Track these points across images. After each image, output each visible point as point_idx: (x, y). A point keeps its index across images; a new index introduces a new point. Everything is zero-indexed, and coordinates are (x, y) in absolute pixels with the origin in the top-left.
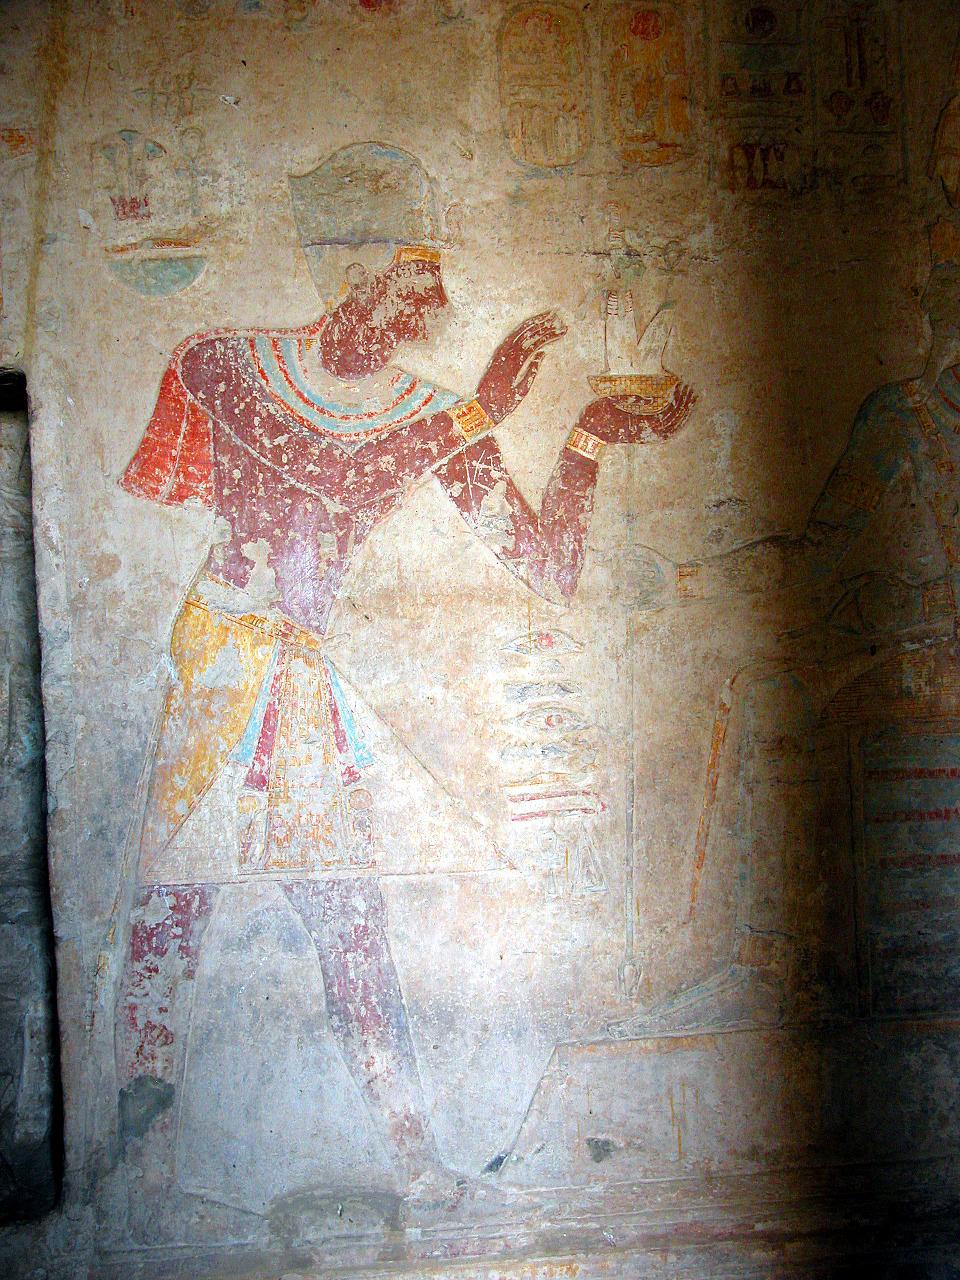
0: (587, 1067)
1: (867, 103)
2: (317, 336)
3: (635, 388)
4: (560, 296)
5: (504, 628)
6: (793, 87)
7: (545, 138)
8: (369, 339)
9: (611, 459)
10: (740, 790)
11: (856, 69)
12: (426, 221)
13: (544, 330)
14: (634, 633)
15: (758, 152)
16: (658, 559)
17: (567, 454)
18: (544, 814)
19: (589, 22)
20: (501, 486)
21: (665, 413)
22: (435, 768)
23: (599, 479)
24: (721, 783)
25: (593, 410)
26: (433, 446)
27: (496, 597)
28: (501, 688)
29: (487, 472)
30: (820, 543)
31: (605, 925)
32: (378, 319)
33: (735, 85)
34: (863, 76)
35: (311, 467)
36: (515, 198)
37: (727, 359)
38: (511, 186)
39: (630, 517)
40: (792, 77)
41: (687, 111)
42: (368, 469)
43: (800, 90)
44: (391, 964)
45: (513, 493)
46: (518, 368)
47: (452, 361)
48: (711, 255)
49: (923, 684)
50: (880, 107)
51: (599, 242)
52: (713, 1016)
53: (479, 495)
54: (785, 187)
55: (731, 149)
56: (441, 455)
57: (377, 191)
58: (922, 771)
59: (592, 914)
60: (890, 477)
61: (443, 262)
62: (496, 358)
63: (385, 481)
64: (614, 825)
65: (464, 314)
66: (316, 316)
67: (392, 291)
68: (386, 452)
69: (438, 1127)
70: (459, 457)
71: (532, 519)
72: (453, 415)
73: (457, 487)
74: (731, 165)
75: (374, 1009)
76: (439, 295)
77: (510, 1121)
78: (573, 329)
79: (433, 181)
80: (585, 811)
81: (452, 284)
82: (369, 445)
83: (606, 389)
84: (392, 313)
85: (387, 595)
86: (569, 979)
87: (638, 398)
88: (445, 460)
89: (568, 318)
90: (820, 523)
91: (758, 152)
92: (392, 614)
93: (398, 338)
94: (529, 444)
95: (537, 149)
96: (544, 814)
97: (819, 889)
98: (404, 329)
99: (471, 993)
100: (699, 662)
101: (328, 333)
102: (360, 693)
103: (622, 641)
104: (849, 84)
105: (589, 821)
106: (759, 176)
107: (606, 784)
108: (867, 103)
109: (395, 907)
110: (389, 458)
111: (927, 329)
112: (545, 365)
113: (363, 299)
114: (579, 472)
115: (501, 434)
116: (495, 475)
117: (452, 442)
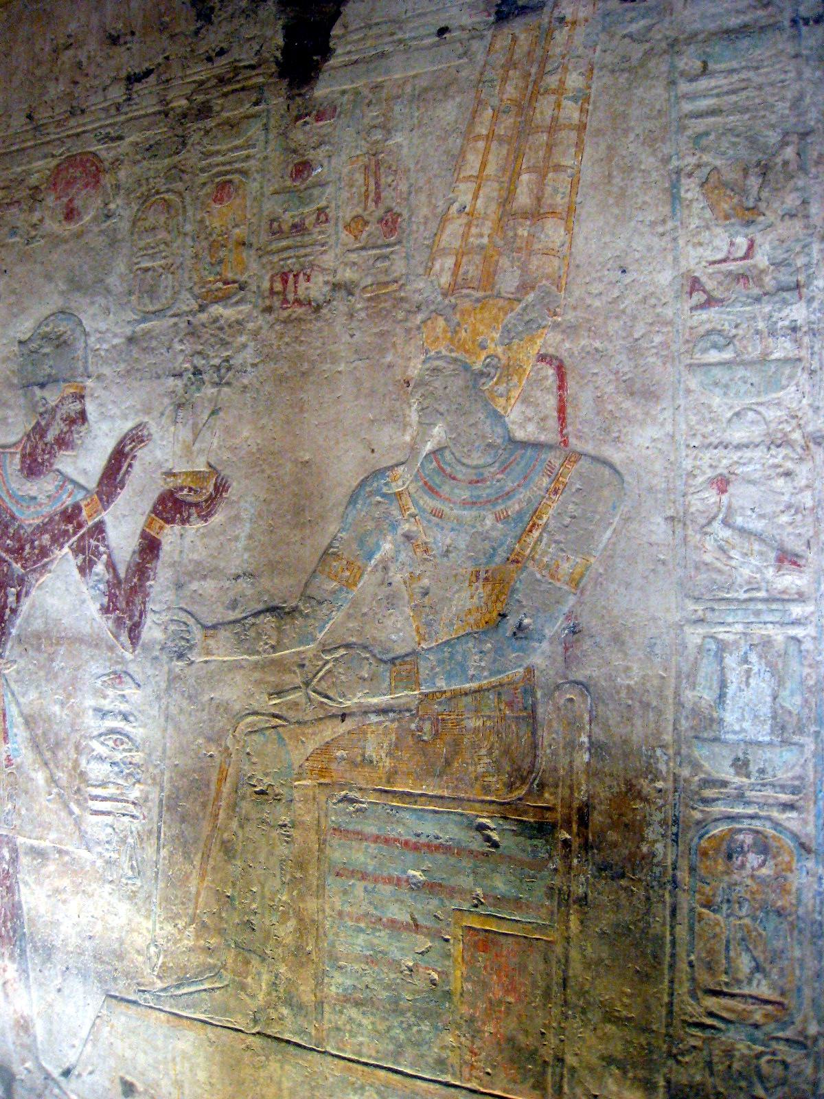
0: (123, 1019)
1: (380, 221)
2: (19, 450)
3: (188, 482)
4: (147, 410)
5: (96, 667)
6: (322, 218)
7: (152, 293)
8: (43, 451)
9: (170, 537)
10: (234, 824)
11: (372, 195)
12: (81, 363)
13: (136, 437)
14: (173, 679)
15: (291, 276)
16: (191, 621)
17: (144, 535)
18: (109, 813)
19: (188, 200)
20: (105, 557)
21: (206, 501)
22: (52, 766)
23: (161, 554)
24: (222, 815)
25: (162, 500)
26: (70, 528)
27: (95, 642)
28: (91, 712)
29: (97, 547)
30: (307, 616)
31: (138, 911)
32: (50, 437)
33: (280, 226)
34: (378, 199)
35: (8, 542)
36: (131, 340)
37: (253, 454)
38: (128, 331)
39: (179, 586)
40: (321, 211)
41: (244, 255)
42: (37, 543)
43: (327, 221)
44: (20, 902)
45: (111, 565)
46: (120, 468)
47: (85, 463)
48: (249, 369)
49: (383, 755)
50: (390, 222)
51: (182, 363)
52: (205, 1007)
53: (91, 564)
54: (309, 303)
55: (272, 281)
56: (75, 533)
57: (58, 346)
58: (378, 837)
59: (130, 898)
60: (370, 559)
61: (87, 392)
62: (109, 461)
63: (44, 552)
64: (150, 832)
65: (95, 427)
66: (19, 437)
67: (58, 416)
68: (46, 531)
69: (39, 1029)
70: (82, 537)
71: (120, 582)
72: (83, 504)
73: (81, 557)
74: (272, 292)
75: (8, 932)
76: (82, 416)
77: (76, 1042)
78: (156, 436)
79: (86, 334)
80: (133, 816)
81: (91, 408)
82: (38, 526)
83: (172, 483)
84: (57, 432)
85: (38, 636)
86: (116, 946)
87: (191, 489)
88: (75, 538)
89: (153, 428)
90: (310, 597)
91: (291, 276)
92: (39, 649)
93: (60, 448)
94: (122, 528)
95: (147, 300)
96: (109, 813)
97: (289, 924)
98: (63, 442)
99: (62, 937)
100: (213, 711)
101: (24, 448)
102: (18, 704)
103: (163, 685)
104: (365, 209)
105: (136, 825)
106: (291, 297)
107: (146, 800)
108: (380, 221)
109: (24, 860)
110: (47, 536)
111: (414, 417)
112: (136, 463)
113: (43, 423)
114: (150, 547)
115: (107, 516)
116: (102, 549)
117: (80, 526)
